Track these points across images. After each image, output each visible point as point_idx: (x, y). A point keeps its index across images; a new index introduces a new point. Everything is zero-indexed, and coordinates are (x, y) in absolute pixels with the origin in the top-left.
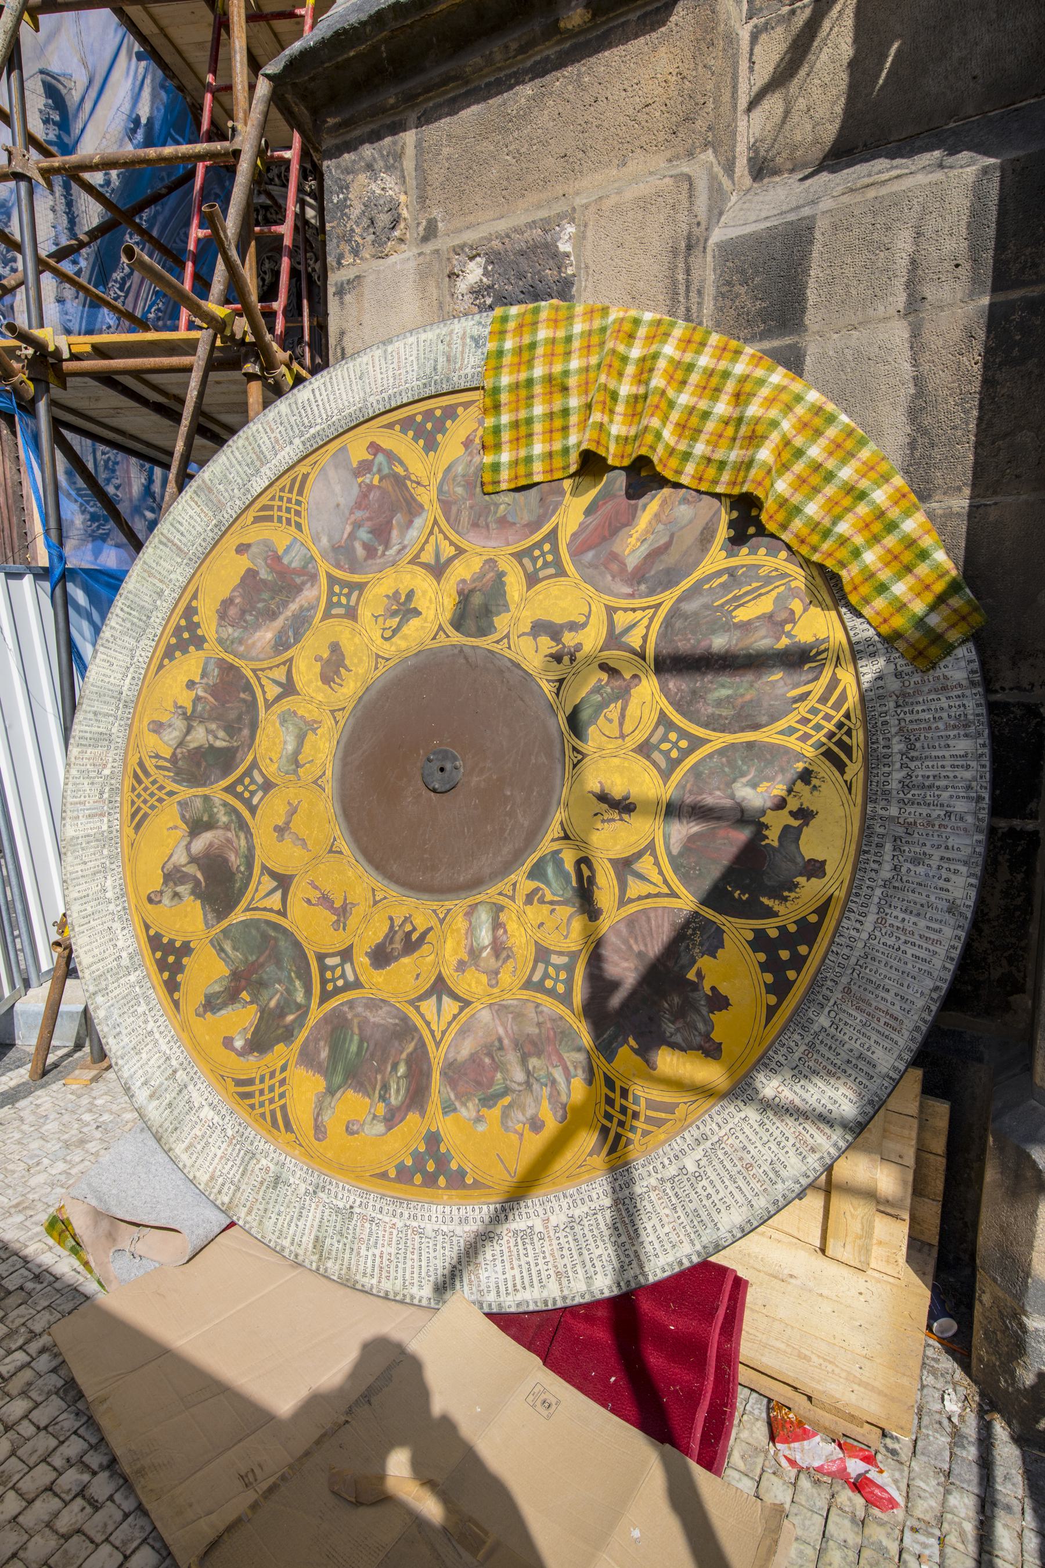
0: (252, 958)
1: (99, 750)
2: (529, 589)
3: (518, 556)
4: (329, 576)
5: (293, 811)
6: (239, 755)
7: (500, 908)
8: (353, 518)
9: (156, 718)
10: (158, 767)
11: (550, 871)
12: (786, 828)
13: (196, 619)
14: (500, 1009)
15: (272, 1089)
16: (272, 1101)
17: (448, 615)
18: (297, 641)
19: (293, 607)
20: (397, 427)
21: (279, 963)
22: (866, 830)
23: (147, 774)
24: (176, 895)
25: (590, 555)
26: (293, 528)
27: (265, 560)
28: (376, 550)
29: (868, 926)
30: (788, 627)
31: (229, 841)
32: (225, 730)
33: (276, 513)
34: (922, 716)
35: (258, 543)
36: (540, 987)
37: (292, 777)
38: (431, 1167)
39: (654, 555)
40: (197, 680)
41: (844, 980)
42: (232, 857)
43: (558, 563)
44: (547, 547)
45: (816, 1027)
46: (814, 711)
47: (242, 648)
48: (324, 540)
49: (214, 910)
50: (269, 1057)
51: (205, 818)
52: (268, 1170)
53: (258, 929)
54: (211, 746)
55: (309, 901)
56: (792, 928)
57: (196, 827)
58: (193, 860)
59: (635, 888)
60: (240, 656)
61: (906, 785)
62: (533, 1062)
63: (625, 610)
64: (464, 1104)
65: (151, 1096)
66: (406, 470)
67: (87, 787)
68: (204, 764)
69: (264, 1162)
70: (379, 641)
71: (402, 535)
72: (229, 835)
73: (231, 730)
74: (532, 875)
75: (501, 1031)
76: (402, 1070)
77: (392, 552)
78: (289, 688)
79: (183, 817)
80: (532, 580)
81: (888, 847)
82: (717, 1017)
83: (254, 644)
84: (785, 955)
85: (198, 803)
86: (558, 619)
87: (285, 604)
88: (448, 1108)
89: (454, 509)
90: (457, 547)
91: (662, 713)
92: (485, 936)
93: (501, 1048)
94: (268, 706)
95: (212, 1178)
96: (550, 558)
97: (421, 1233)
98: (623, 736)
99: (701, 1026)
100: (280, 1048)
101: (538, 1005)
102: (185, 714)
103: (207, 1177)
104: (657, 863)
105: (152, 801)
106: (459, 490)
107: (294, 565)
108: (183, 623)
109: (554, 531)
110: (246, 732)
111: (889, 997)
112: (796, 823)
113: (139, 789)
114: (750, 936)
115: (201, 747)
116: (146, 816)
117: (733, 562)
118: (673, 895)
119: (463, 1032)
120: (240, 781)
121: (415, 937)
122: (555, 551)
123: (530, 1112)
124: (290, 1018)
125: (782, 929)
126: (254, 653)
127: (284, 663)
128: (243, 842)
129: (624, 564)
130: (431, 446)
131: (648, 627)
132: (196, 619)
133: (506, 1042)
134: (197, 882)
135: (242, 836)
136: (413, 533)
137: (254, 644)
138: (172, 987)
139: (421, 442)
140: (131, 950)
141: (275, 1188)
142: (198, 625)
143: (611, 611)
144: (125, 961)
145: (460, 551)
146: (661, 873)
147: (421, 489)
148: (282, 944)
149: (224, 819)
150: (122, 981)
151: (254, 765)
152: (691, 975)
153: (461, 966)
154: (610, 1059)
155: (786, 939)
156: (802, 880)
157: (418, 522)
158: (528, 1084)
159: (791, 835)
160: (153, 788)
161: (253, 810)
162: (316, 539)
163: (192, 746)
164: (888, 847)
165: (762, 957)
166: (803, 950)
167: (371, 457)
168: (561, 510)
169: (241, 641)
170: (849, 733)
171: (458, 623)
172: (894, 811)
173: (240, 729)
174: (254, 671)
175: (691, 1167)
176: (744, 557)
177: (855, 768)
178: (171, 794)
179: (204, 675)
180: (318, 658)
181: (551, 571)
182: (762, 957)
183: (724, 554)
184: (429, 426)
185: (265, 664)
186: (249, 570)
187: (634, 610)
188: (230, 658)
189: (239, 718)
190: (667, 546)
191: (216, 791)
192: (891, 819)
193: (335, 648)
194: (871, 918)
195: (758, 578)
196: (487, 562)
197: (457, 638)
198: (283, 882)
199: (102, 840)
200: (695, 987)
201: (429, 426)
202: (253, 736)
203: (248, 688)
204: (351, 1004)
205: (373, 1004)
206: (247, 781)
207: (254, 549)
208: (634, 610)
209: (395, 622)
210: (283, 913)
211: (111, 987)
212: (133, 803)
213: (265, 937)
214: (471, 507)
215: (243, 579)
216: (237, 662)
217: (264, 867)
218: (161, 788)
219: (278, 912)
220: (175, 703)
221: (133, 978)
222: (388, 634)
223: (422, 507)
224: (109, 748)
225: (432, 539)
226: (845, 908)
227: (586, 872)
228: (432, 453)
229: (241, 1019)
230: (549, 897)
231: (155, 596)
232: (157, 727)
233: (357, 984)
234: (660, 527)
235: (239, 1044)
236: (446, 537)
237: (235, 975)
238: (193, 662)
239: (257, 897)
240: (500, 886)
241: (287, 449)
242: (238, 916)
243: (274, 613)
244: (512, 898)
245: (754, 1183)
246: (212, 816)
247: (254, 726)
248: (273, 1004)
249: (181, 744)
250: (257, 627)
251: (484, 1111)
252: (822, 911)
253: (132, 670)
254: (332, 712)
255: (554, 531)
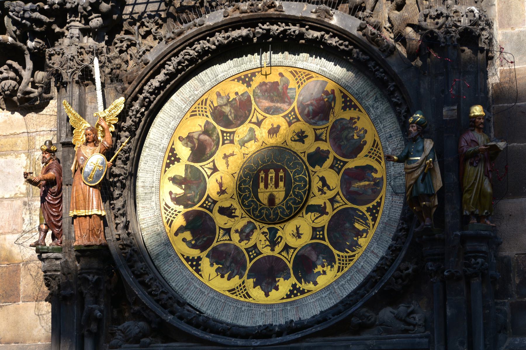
0: (192, 179)
1: (199, 84)
2: (329, 168)
3: (335, 158)
4: (294, 108)
5: (232, 155)
6: (232, 126)
7: (256, 229)
8: (312, 101)
9: (221, 92)
10: (210, 106)
11: (273, 232)
12: (320, 272)
13: (253, 78)
14: (236, 248)
15: (173, 214)
16: (171, 216)
17: (309, 152)
18: (272, 114)
19: (279, 105)
20: (342, 94)
21: (198, 187)
22: (328, 286)
23: (205, 105)
24: (187, 143)
25: (346, 177)
26: (297, 85)
27: (284, 84)
28: (310, 116)
29: (312, 301)
30: (359, 237)
31: (211, 144)
32: (235, 115)
33: (297, 77)
34: (357, 278)
35: (286, 78)
36: (248, 252)
37: (240, 147)
38: (194, 263)
39: (356, 193)
40: (240, 94)
41: (299, 305)
42: (208, 150)
43: (340, 170)
44: (342, 164)
45: (286, 308)
46: (346, 257)
47: (257, 100)
48: (301, 98)
49: (193, 158)
50: (177, 206)
51: (210, 132)
52: (158, 230)
53: (200, 174)
54: (227, 115)
55: (217, 181)
56: (301, 289)
57: (206, 132)
58: (198, 139)
59: (284, 253)
60: (255, 101)
61: (342, 285)
62: (233, 265)
63: (340, 197)
64: (212, 258)
65: (143, 187)
66: (334, 106)
67: (187, 90)
68: (222, 118)
69: (159, 228)
70: (289, 138)
71: (319, 120)
72: (212, 143)
73: (236, 117)
74: (268, 229)
75: (233, 252)
76: (205, 239)
77: (313, 121)
78: (259, 124)
79: (205, 126)
80: (332, 167)
81: (329, 292)
82: (274, 291)
83: (261, 102)
84: (295, 292)
85: (212, 126)
86: (328, 182)
87: (278, 102)
88: (207, 256)
89: (333, 130)
90: (326, 139)
91: (324, 226)
92: (247, 231)
93: (229, 255)
94: (250, 122)
95: (144, 219)
96: (340, 167)
97: (182, 273)
98: (313, 222)
99: (269, 289)
100: (182, 207)
101: (244, 255)
102: (229, 99)
103: (143, 218)
104: (293, 253)
105: (201, 113)
106: (339, 127)
107: (289, 95)
108: (249, 75)
109: (347, 162)
110: (239, 122)
111: (302, 314)
112: (322, 272)
113: (200, 106)
114: (294, 283)
115: (224, 112)
116: (196, 115)
117: (366, 213)
118: (290, 262)
119: (225, 245)
120: (227, 133)
121: (233, 214)
122: (342, 166)
123: (223, 273)
124: (190, 202)
125: (300, 287)
126: (259, 104)
127: (264, 116)
128: (214, 149)
129: (350, 188)
130: (344, 109)
131: (340, 206)
132: (253, 78)
133: (231, 255)
134: (195, 147)
135: (215, 147)
136: (321, 123)
137: (261, 102)
138: (168, 166)
139: (343, 105)
140: (165, 146)
141: (157, 235)
142: (252, 80)
143: (338, 194)
144: (161, 147)
145: (326, 141)
146: (292, 256)
147: (332, 115)
148: (202, 184)
149: (215, 138)
150: (156, 151)
151: (234, 133)
152: (277, 279)
153: (237, 231)
154: (248, 278)
155: (298, 290)
156: (311, 283)
157: (324, 122)
158: (228, 267)
159: (319, 274)
160: (204, 110)
161: (223, 144)
162: (300, 95)
163: (223, 110)
164: (329, 292)
165: (292, 288)
166: (299, 294)
167: (330, 93)
168: (352, 160)
169: (258, 98)
170: (346, 267)
171: (310, 157)
172: (336, 287)
173: (238, 120)
174: (255, 109)
175: (243, 309)
176: (368, 214)
177: (340, 274)
178: (207, 116)
179: (242, 95)
180: (272, 125)
181: (337, 170)
182: (292, 288)
183: (366, 209)
184: (348, 104)
185: (259, 111)
186: (277, 82)
187: (342, 199)
188: (252, 98)
189: (241, 117)
190: (360, 194)
191: (219, 128)
192: (334, 288)
193: (279, 127)
194: (314, 300)
195: (365, 221)
196: (328, 150)
197: (305, 159)
198: (215, 169)
199: (180, 110)
200: (276, 282)
201: (348, 104)
202: (239, 125)
203: (250, 112)
204: (206, 214)
205: (212, 219)
206: (228, 135)
207: (283, 78)
208: (342, 199)
209: (297, 138)
210: (209, 177)
211: (152, 150)
212: (196, 108)
213: (199, 178)
214: (337, 134)
215: (274, 82)
216: (253, 102)
217: (213, 161)
218: (206, 112)
219: (208, 175)
220: (228, 94)
221: (160, 153)
222: (293, 139)
223: (329, 119)
224: (202, 87)
225: (323, 130)
226: (312, 295)
227: (279, 240)
228: (342, 110)
229: (179, 191)
230: (268, 237)
231: (249, 60)
232: (219, 95)
233: (211, 211)
234: (363, 189)
235: (173, 196)
236: (326, 134)
237: (185, 179)
238: (243, 88)
239: (206, 166)
240: (260, 224)
241: (315, 65)
242: (197, 165)
243: (273, 100)
244: (260, 229)
245: (251, 322)
246: (212, 133)
247: (242, 123)
248: (188, 195)
249: (221, 106)
250: (266, 99)
251: (214, 264)
252: (309, 291)
253: (226, 73)
254: (263, 142)
255: (347, 162)
